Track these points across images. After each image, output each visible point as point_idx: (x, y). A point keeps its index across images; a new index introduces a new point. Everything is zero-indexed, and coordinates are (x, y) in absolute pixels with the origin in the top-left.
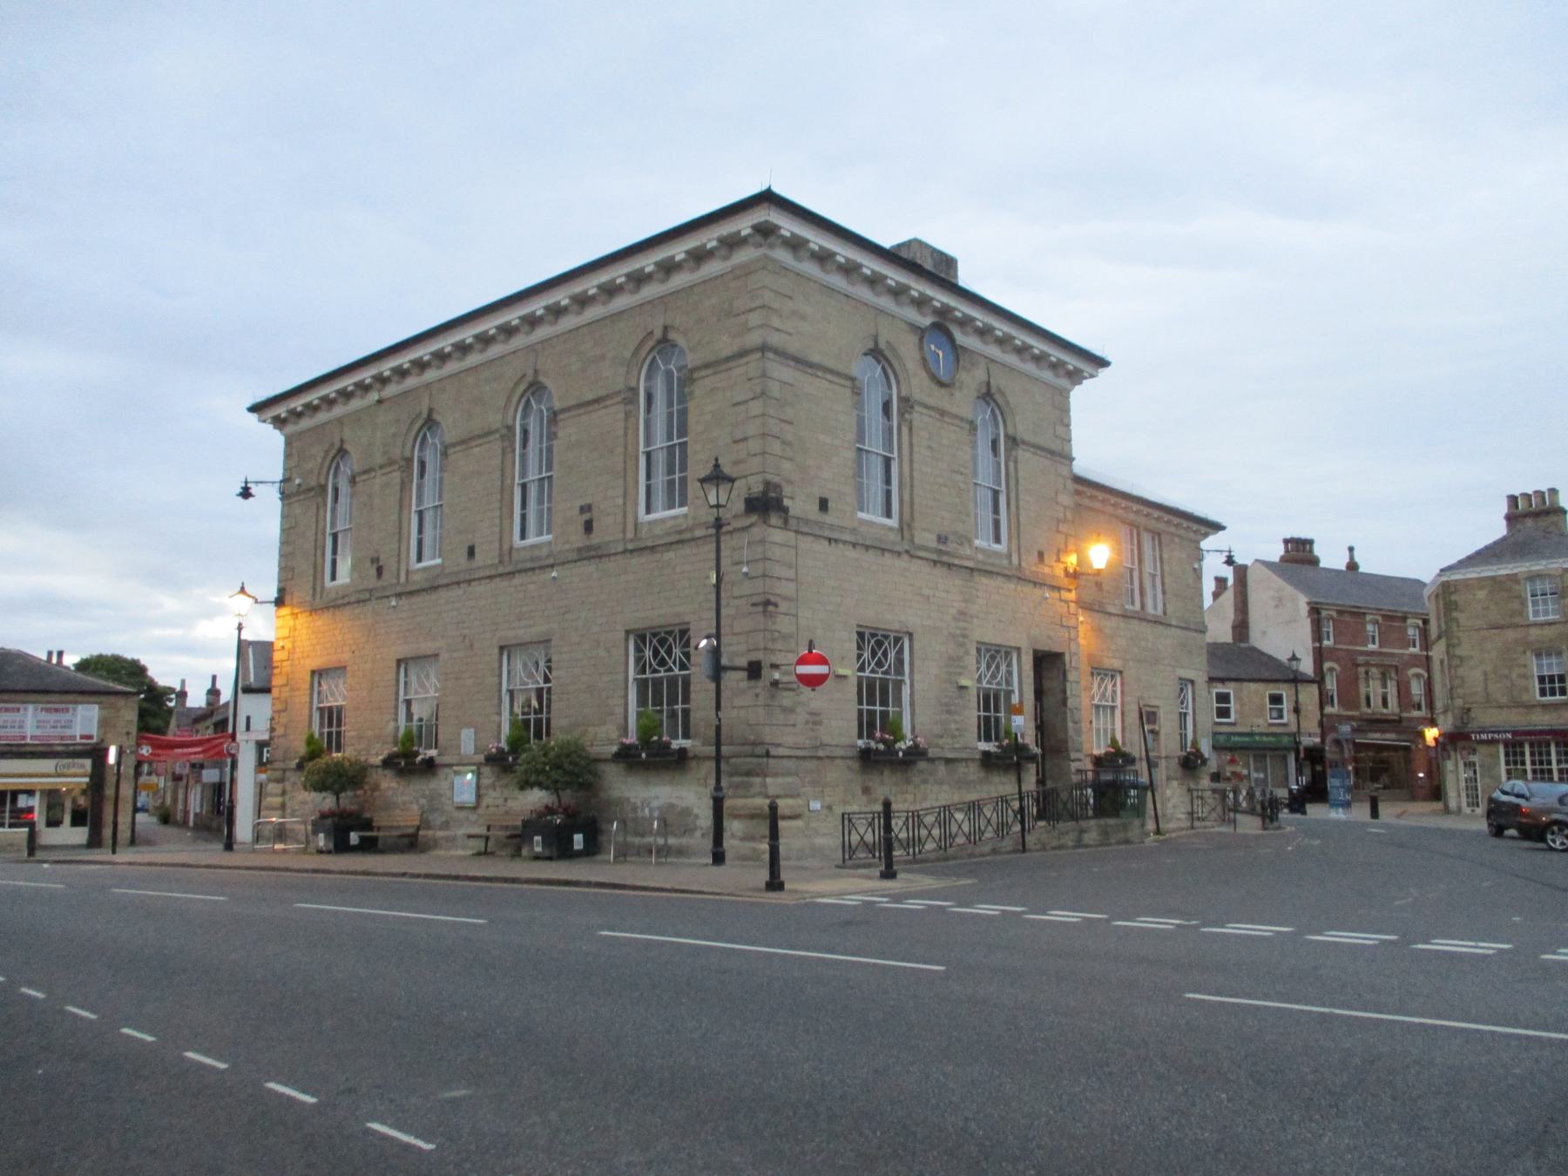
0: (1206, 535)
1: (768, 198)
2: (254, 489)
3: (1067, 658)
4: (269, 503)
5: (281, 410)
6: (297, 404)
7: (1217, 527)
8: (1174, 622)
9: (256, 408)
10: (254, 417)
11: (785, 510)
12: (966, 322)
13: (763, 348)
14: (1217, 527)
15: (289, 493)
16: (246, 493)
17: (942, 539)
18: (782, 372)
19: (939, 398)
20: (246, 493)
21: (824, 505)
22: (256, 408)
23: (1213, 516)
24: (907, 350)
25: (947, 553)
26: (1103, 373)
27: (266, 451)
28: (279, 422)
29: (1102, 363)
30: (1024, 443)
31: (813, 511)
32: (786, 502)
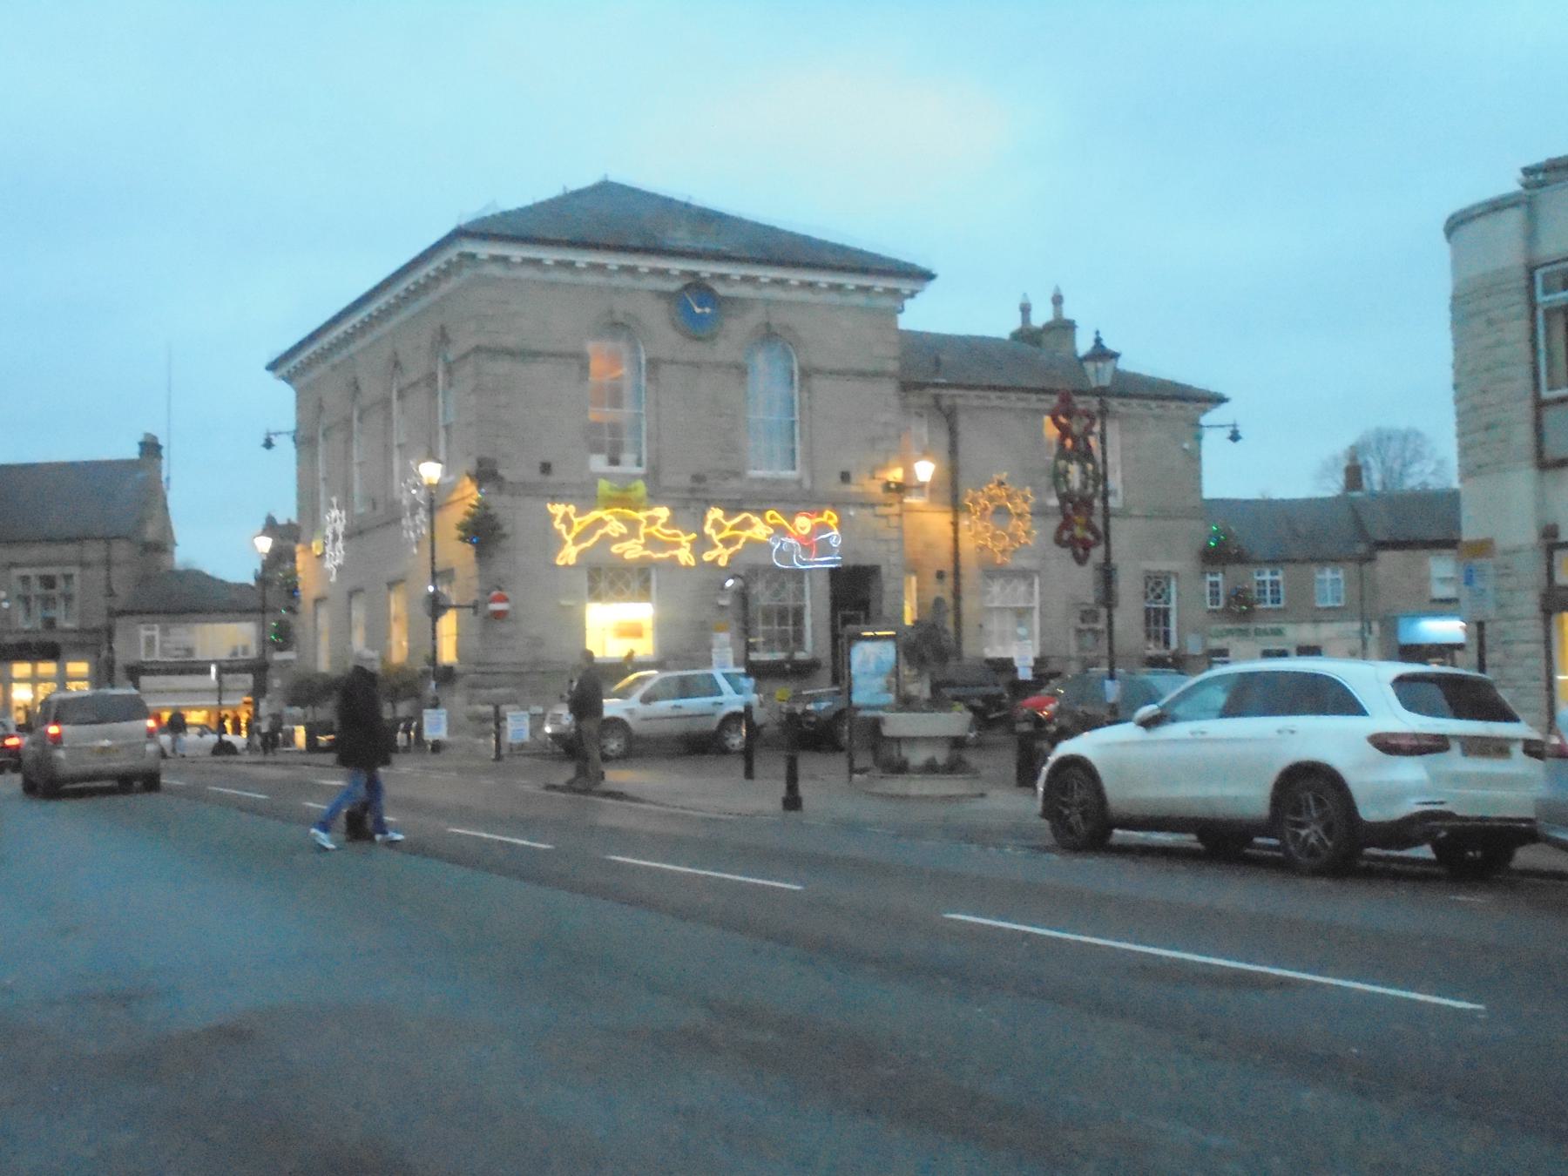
0: (1205, 411)
1: (460, 234)
2: (275, 440)
3: (884, 570)
4: (286, 449)
5: (283, 371)
6: (295, 362)
7: (1219, 400)
8: (1135, 512)
9: (273, 366)
10: (269, 375)
11: (501, 479)
12: (723, 278)
13: (478, 349)
14: (1219, 400)
15: (305, 441)
16: (268, 444)
17: (698, 478)
18: (503, 367)
19: (693, 351)
20: (268, 444)
21: (546, 468)
22: (273, 366)
23: (1215, 387)
24: (655, 316)
25: (704, 490)
26: (931, 287)
27: (279, 404)
28: (289, 379)
29: (927, 276)
30: (818, 371)
31: (535, 476)
32: (501, 472)
